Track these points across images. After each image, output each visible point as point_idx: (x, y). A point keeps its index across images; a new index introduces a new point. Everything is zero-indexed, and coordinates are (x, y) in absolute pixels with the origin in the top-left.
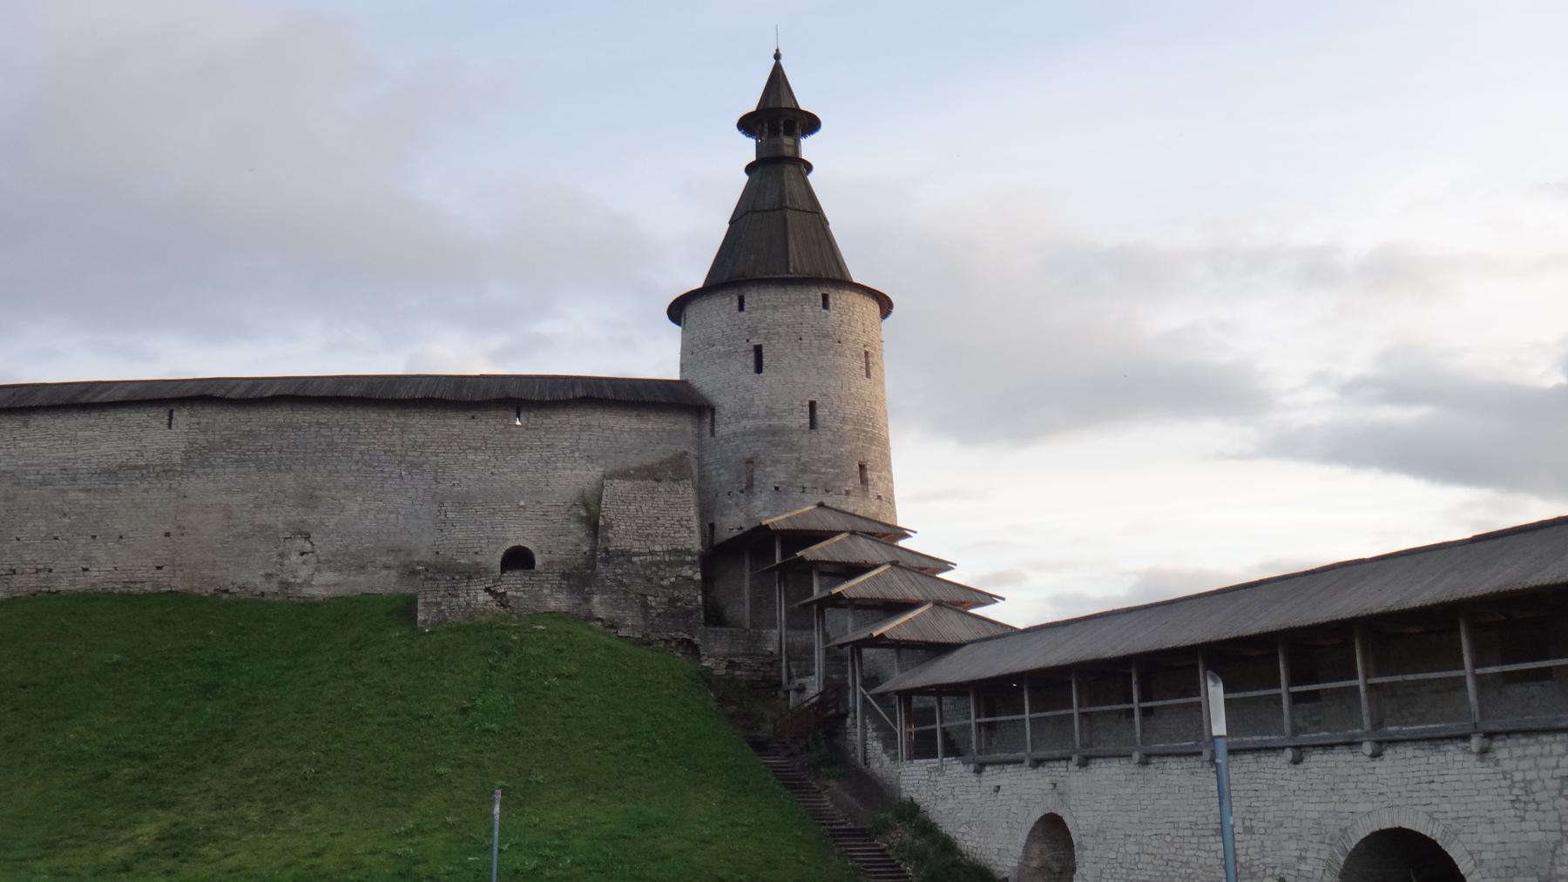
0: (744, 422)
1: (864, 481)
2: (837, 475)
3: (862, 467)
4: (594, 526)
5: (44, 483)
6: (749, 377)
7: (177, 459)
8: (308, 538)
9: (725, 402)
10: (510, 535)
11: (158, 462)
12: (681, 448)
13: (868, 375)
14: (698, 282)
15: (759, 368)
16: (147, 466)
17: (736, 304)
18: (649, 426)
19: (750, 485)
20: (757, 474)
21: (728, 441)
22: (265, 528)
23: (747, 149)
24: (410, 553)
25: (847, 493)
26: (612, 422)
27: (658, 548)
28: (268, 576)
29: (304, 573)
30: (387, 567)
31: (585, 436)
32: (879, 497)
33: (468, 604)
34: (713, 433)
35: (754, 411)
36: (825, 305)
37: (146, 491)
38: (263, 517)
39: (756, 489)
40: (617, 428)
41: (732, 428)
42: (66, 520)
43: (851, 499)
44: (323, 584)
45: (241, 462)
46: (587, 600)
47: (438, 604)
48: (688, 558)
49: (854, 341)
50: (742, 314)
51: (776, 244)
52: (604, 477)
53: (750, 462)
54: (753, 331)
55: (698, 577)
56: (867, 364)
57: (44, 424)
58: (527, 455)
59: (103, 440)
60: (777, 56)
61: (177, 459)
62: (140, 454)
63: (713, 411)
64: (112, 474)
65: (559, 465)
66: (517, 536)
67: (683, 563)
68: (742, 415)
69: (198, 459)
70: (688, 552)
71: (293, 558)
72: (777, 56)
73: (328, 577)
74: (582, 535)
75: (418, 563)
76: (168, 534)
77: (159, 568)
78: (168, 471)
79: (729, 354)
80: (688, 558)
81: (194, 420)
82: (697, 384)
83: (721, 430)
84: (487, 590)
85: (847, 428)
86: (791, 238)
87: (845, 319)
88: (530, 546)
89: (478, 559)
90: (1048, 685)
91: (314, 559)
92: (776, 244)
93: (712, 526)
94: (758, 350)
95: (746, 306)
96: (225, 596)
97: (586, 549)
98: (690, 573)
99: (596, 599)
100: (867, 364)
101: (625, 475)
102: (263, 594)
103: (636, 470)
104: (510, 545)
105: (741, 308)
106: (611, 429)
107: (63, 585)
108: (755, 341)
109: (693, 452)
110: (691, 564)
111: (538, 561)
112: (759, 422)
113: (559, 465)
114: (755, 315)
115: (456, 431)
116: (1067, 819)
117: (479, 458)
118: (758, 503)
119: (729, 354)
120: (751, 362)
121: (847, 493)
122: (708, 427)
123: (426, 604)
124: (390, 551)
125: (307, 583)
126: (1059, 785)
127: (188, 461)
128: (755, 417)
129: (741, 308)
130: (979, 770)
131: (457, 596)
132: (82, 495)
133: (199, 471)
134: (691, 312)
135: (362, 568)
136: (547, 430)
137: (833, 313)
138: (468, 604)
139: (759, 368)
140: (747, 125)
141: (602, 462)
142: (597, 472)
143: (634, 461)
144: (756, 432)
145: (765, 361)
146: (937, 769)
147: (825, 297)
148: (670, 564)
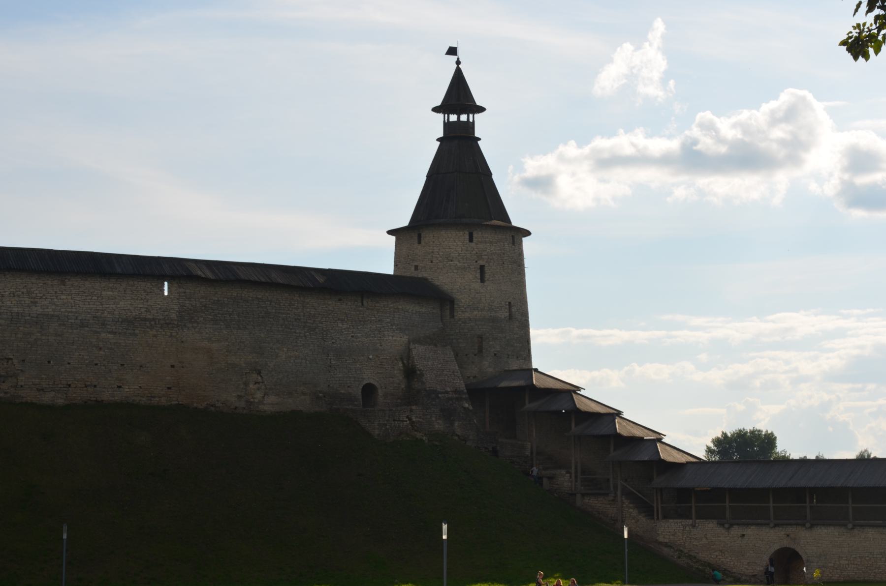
0: (475, 313)
4: (410, 373)
6: (477, 285)
7: (174, 316)
8: (259, 373)
11: (161, 317)
15: (482, 280)
16: (154, 319)
17: (467, 237)
18: (423, 310)
19: (480, 350)
27: (449, 389)
28: (239, 397)
30: (304, 394)
34: (452, 316)
37: (155, 336)
41: (467, 315)
42: (101, 352)
44: (270, 404)
47: (385, 425)
50: (473, 244)
51: (460, 191)
52: (409, 342)
57: (76, 284)
59: (120, 299)
61: (174, 316)
66: (369, 376)
71: (251, 386)
73: (272, 399)
74: (401, 378)
75: (320, 392)
76: (173, 366)
77: (169, 388)
81: (182, 290)
83: (459, 315)
88: (375, 383)
90: (798, 494)
91: (263, 387)
92: (460, 191)
94: (482, 268)
95: (474, 240)
96: (213, 409)
97: (403, 386)
98: (467, 405)
99: (456, 424)
101: (418, 341)
102: (236, 408)
104: (365, 382)
105: (471, 240)
107: (106, 396)
108: (481, 263)
115: (330, 308)
117: (345, 326)
120: (478, 275)
122: (448, 313)
129: (471, 240)
132: (110, 336)
133: (190, 325)
139: (482, 280)
142: (405, 339)
145: (487, 276)
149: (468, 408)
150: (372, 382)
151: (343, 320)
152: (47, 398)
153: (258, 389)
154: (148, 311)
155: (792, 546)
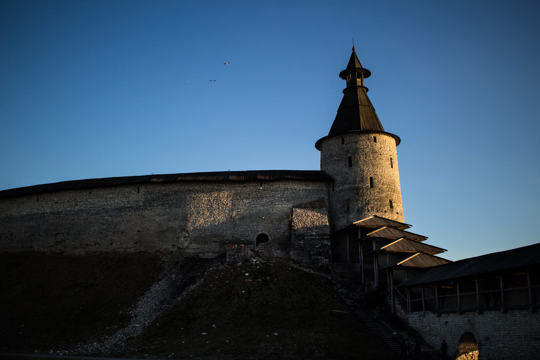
0: (345, 186)
1: (392, 207)
3: (391, 202)
5: (97, 214)
6: (346, 169)
9: (339, 178)
10: (259, 230)
11: (134, 205)
12: (322, 196)
13: (392, 167)
14: (326, 134)
15: (350, 165)
16: (131, 207)
17: (341, 141)
18: (310, 188)
19: (348, 209)
20: (351, 205)
21: (339, 193)
22: (172, 228)
23: (343, 84)
24: (223, 237)
25: (385, 211)
26: (296, 187)
27: (314, 233)
28: (174, 246)
29: (186, 244)
30: (215, 242)
31: (286, 192)
32: (398, 213)
33: (245, 255)
34: (333, 190)
35: (349, 181)
36: (375, 141)
37: (131, 216)
38: (171, 224)
39: (351, 211)
40: (298, 189)
42: (104, 227)
43: (387, 214)
45: (163, 205)
46: (288, 253)
48: (326, 237)
52: (293, 207)
53: (348, 200)
54: (348, 152)
55: (329, 244)
56: (392, 162)
57: (96, 193)
58: (265, 200)
60: (353, 49)
62: (129, 203)
63: (333, 182)
64: (119, 210)
65: (277, 203)
66: (261, 229)
67: (324, 239)
68: (344, 183)
69: (149, 203)
70: (325, 235)
71: (182, 239)
72: (353, 49)
73: (194, 246)
74: (286, 229)
75: (226, 240)
76: (139, 231)
77: (136, 243)
78: (138, 208)
79: (339, 160)
80: (326, 237)
81: (147, 190)
82: (327, 172)
83: (337, 189)
84: (251, 250)
85: (384, 187)
86: (361, 117)
87: (383, 146)
88: (267, 233)
89: (248, 238)
91: (189, 239)
93: (334, 225)
94: (350, 158)
95: (345, 142)
98: (326, 243)
99: (292, 253)
100: (392, 162)
103: (306, 204)
104: (259, 233)
105: (343, 143)
106: (296, 189)
108: (349, 155)
109: (326, 197)
110: (327, 239)
111: (270, 238)
112: (351, 185)
113: (277, 203)
114: (349, 145)
115: (239, 192)
116: (474, 334)
118: (351, 216)
119: (339, 160)
120: (347, 163)
121: (385, 211)
123: (229, 255)
124: (216, 236)
125: (187, 248)
126: (471, 321)
127: (145, 205)
128: (349, 184)
129: (343, 143)
130: (439, 316)
131: (240, 252)
132: (109, 218)
133: (149, 208)
134: (324, 144)
135: (206, 242)
136: (272, 191)
137: (378, 145)
138: (245, 255)
140: (343, 75)
141: (292, 202)
143: (305, 201)
144: (350, 189)
145: (353, 163)
146: (422, 315)
147: (375, 138)
148: (319, 239)
149: (327, 245)
150: (264, 232)
151: (247, 198)
152: (77, 252)
153: (186, 241)
154: (129, 203)
155: (472, 332)
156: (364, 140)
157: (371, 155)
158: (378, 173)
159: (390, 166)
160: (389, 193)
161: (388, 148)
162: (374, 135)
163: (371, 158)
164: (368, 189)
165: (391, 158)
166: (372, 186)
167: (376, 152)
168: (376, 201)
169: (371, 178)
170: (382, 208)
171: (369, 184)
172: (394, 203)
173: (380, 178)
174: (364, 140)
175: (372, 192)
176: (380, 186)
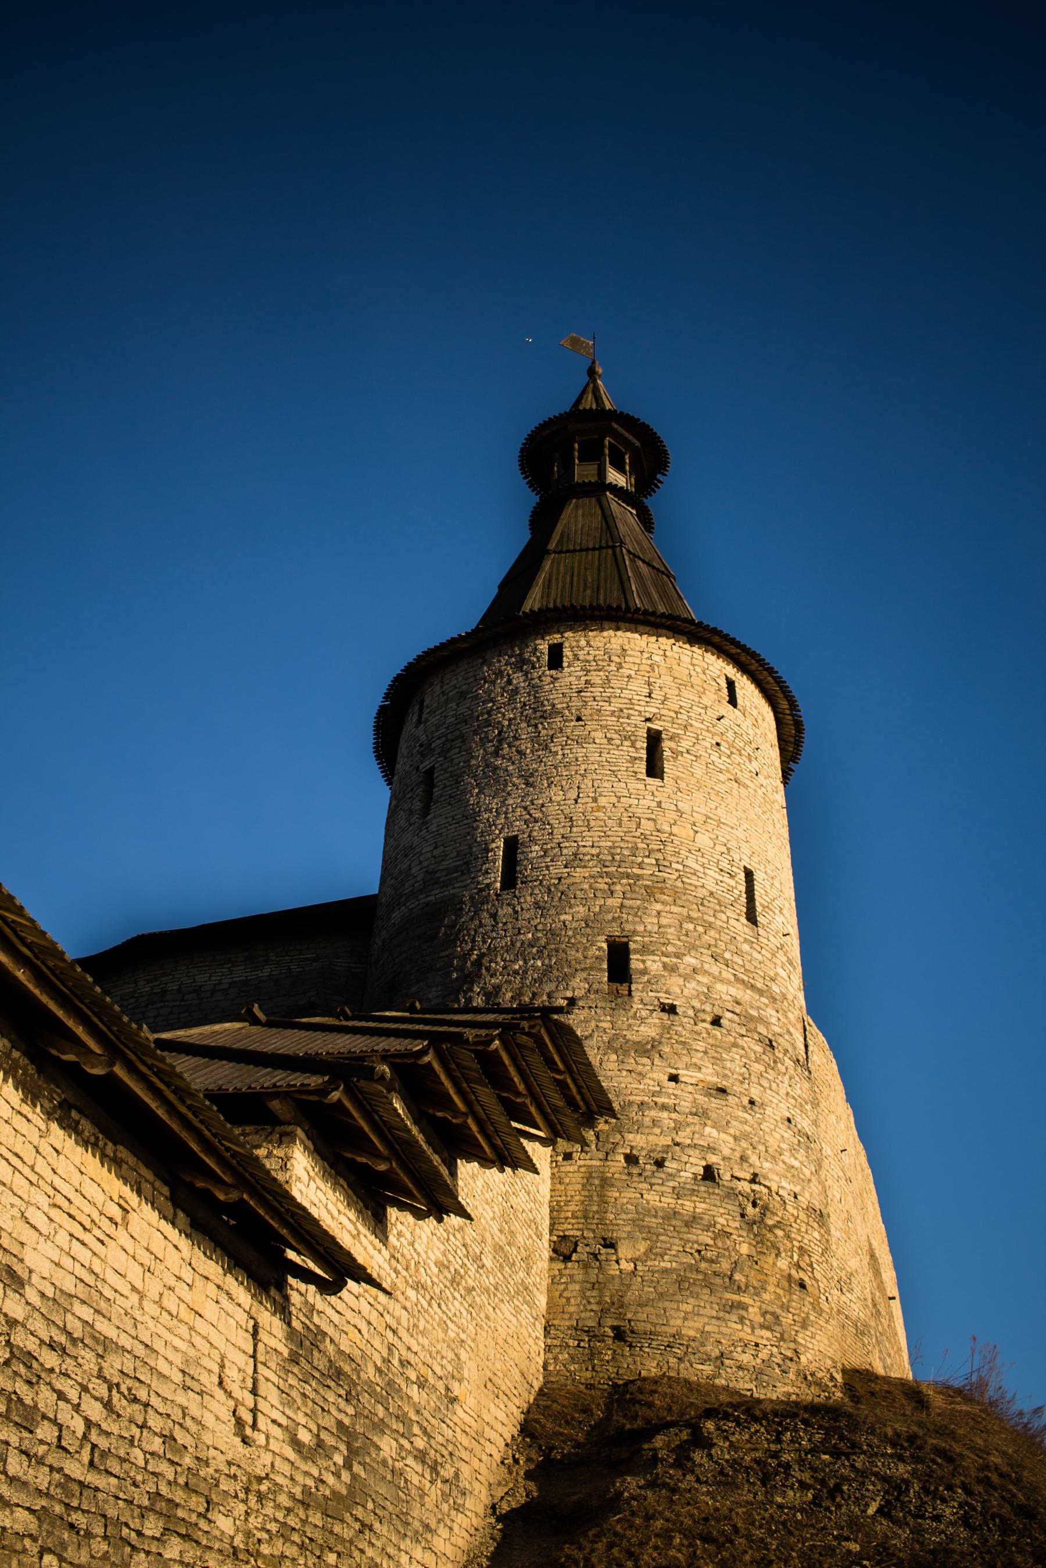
2: (548, 970)
13: (655, 769)
36: (556, 659)
49: (618, 714)
87: (596, 678)
137: (571, 675)
156: (500, 674)
157: (525, 731)
158: (552, 809)
159: (642, 767)
160: (613, 902)
161: (638, 687)
162: (556, 638)
163: (526, 746)
164: (486, 900)
165: (654, 740)
166: (510, 880)
167: (555, 712)
168: (522, 954)
169: (512, 845)
170: (549, 987)
171: (495, 878)
172: (645, 950)
173: (559, 832)
174: (500, 674)
175: (504, 911)
176: (558, 869)
